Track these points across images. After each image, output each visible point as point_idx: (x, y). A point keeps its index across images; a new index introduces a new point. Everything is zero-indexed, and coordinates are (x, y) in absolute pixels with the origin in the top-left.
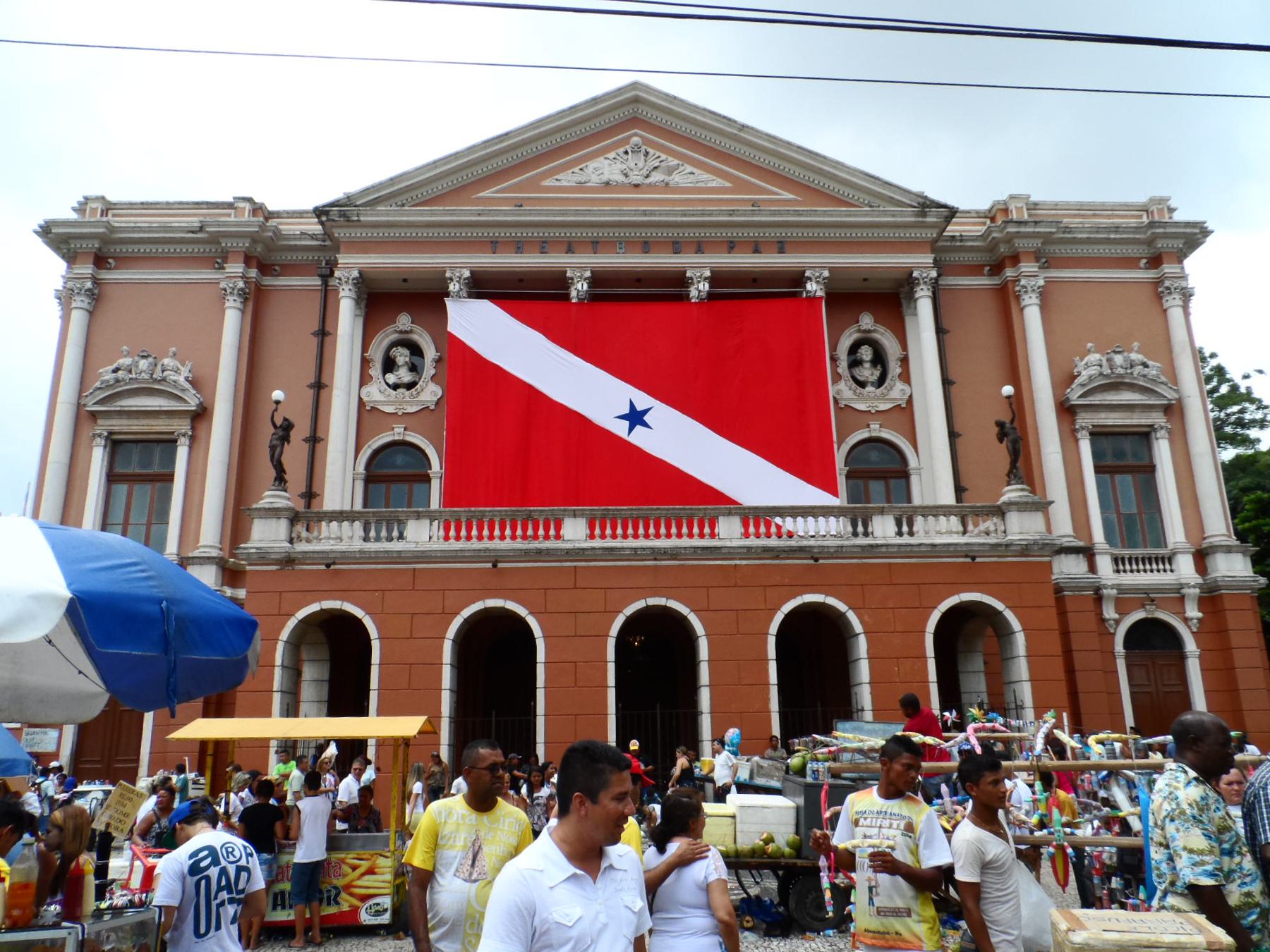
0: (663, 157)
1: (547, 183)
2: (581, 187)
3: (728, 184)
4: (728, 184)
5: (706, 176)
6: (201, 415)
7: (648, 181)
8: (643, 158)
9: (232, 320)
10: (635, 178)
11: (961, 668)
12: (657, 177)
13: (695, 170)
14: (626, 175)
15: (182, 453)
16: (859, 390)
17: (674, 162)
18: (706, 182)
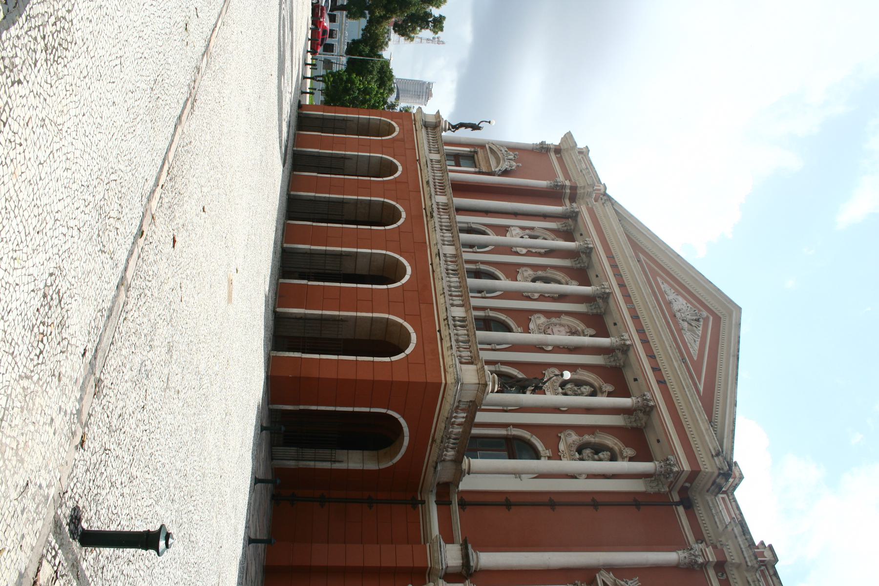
0: (701, 328)
1: (659, 279)
2: (663, 294)
3: (695, 358)
4: (695, 358)
5: (697, 347)
6: (491, 173)
7: (681, 321)
8: (694, 318)
9: (542, 183)
10: (678, 315)
11: (366, 453)
12: (685, 325)
13: (698, 343)
14: (680, 310)
15: (472, 169)
16: (574, 449)
17: (700, 333)
18: (693, 347)
